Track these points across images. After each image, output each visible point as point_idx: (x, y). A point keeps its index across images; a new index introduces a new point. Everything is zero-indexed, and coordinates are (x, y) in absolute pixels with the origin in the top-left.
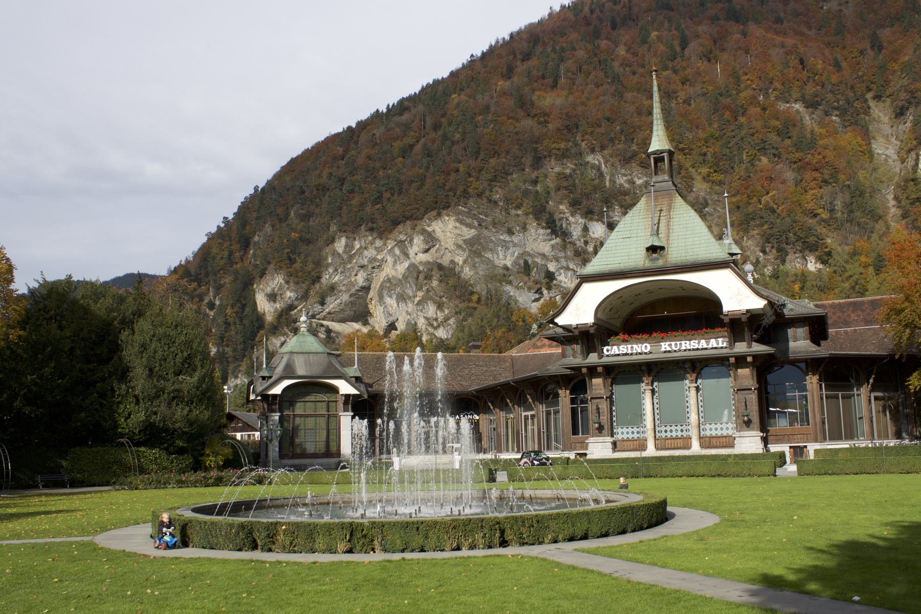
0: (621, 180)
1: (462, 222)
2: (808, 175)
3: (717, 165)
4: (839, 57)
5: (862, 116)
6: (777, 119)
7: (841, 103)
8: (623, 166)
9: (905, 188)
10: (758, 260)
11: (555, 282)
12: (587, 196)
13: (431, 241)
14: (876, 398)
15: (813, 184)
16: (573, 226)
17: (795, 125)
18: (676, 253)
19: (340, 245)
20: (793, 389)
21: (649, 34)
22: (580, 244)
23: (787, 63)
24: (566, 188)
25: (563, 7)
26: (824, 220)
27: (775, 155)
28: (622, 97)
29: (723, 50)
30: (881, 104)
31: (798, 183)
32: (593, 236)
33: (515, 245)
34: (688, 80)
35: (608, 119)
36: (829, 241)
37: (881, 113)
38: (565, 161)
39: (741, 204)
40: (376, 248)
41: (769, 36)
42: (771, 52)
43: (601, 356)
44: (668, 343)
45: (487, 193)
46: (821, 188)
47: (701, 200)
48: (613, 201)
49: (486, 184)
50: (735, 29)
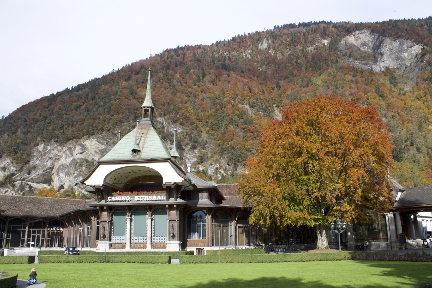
0: (171, 130)
1: (99, 142)
2: (249, 134)
3: (212, 127)
5: (271, 113)
7: (264, 107)
8: (173, 124)
10: (226, 168)
13: (84, 149)
14: (239, 227)
15: (250, 138)
17: (245, 114)
18: (144, 155)
19: (41, 147)
21: (190, 70)
23: (244, 89)
25: (156, 55)
27: (236, 125)
28: (175, 95)
29: (219, 81)
31: (244, 137)
34: (204, 91)
35: (168, 103)
39: (220, 144)
40: (58, 150)
41: (238, 77)
42: (238, 83)
43: (107, 201)
44: (138, 197)
45: (112, 130)
47: (205, 141)
48: (167, 138)
49: (112, 126)
50: (225, 73)
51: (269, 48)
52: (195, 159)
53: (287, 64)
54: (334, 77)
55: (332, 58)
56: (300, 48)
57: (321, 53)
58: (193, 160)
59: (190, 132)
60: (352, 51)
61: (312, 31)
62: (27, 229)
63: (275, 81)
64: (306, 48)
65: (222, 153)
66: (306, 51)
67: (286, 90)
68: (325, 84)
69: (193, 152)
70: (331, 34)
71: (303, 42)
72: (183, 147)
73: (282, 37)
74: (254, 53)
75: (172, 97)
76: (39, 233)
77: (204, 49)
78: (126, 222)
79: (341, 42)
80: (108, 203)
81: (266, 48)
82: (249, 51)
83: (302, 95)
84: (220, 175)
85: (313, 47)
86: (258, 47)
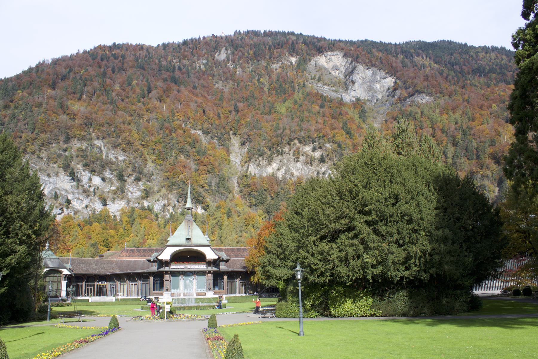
0: (111, 156)
2: (202, 167)
3: (160, 155)
4: (221, 113)
5: (227, 142)
6: (190, 138)
8: (113, 149)
9: (242, 179)
10: (175, 205)
11: (71, 205)
12: (93, 162)
15: (203, 172)
16: (84, 177)
17: (197, 142)
18: (194, 241)
20: (220, 279)
21: (132, 81)
22: (86, 186)
23: (197, 111)
24: (82, 156)
25: (85, 52)
26: (207, 190)
28: (116, 113)
29: (168, 96)
30: (235, 137)
32: (94, 183)
33: (51, 183)
35: (108, 124)
36: (208, 200)
37: (235, 141)
38: (83, 141)
39: (169, 177)
41: (190, 95)
42: (191, 104)
45: (38, 153)
46: (206, 174)
47: (150, 172)
48: (106, 166)
49: (37, 147)
50: (175, 87)
51: (228, 60)
52: (139, 193)
53: (247, 82)
54: (300, 106)
55: (299, 81)
56: (264, 64)
57: (287, 73)
58: (136, 194)
59: (134, 161)
60: (322, 75)
61: (278, 45)
62: (84, 283)
63: (233, 102)
64: (271, 64)
65: (170, 187)
66: (271, 69)
67: (244, 116)
68: (290, 114)
69: (137, 185)
70: (300, 51)
71: (267, 57)
72: (126, 178)
73: (244, 48)
74: (210, 64)
75: (113, 116)
76: (91, 285)
77: (147, 51)
78: (182, 281)
79: (310, 62)
80: (171, 270)
81: (224, 60)
82: (204, 62)
83: (263, 124)
84: (169, 213)
85: (278, 65)
86: (214, 57)
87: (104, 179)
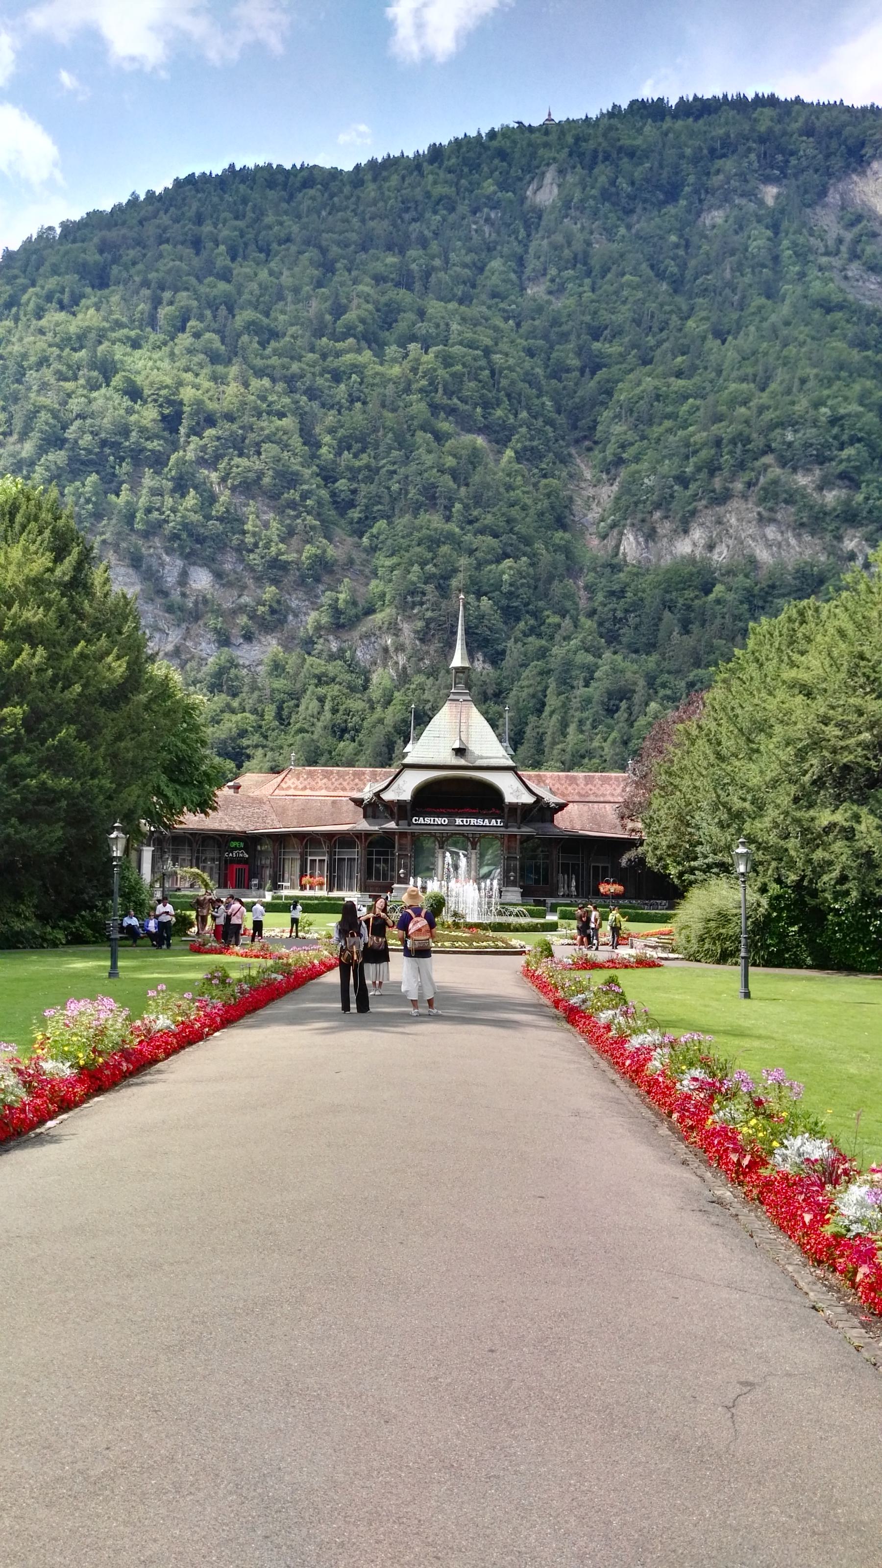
43: (410, 824)
87: (218, 575)
